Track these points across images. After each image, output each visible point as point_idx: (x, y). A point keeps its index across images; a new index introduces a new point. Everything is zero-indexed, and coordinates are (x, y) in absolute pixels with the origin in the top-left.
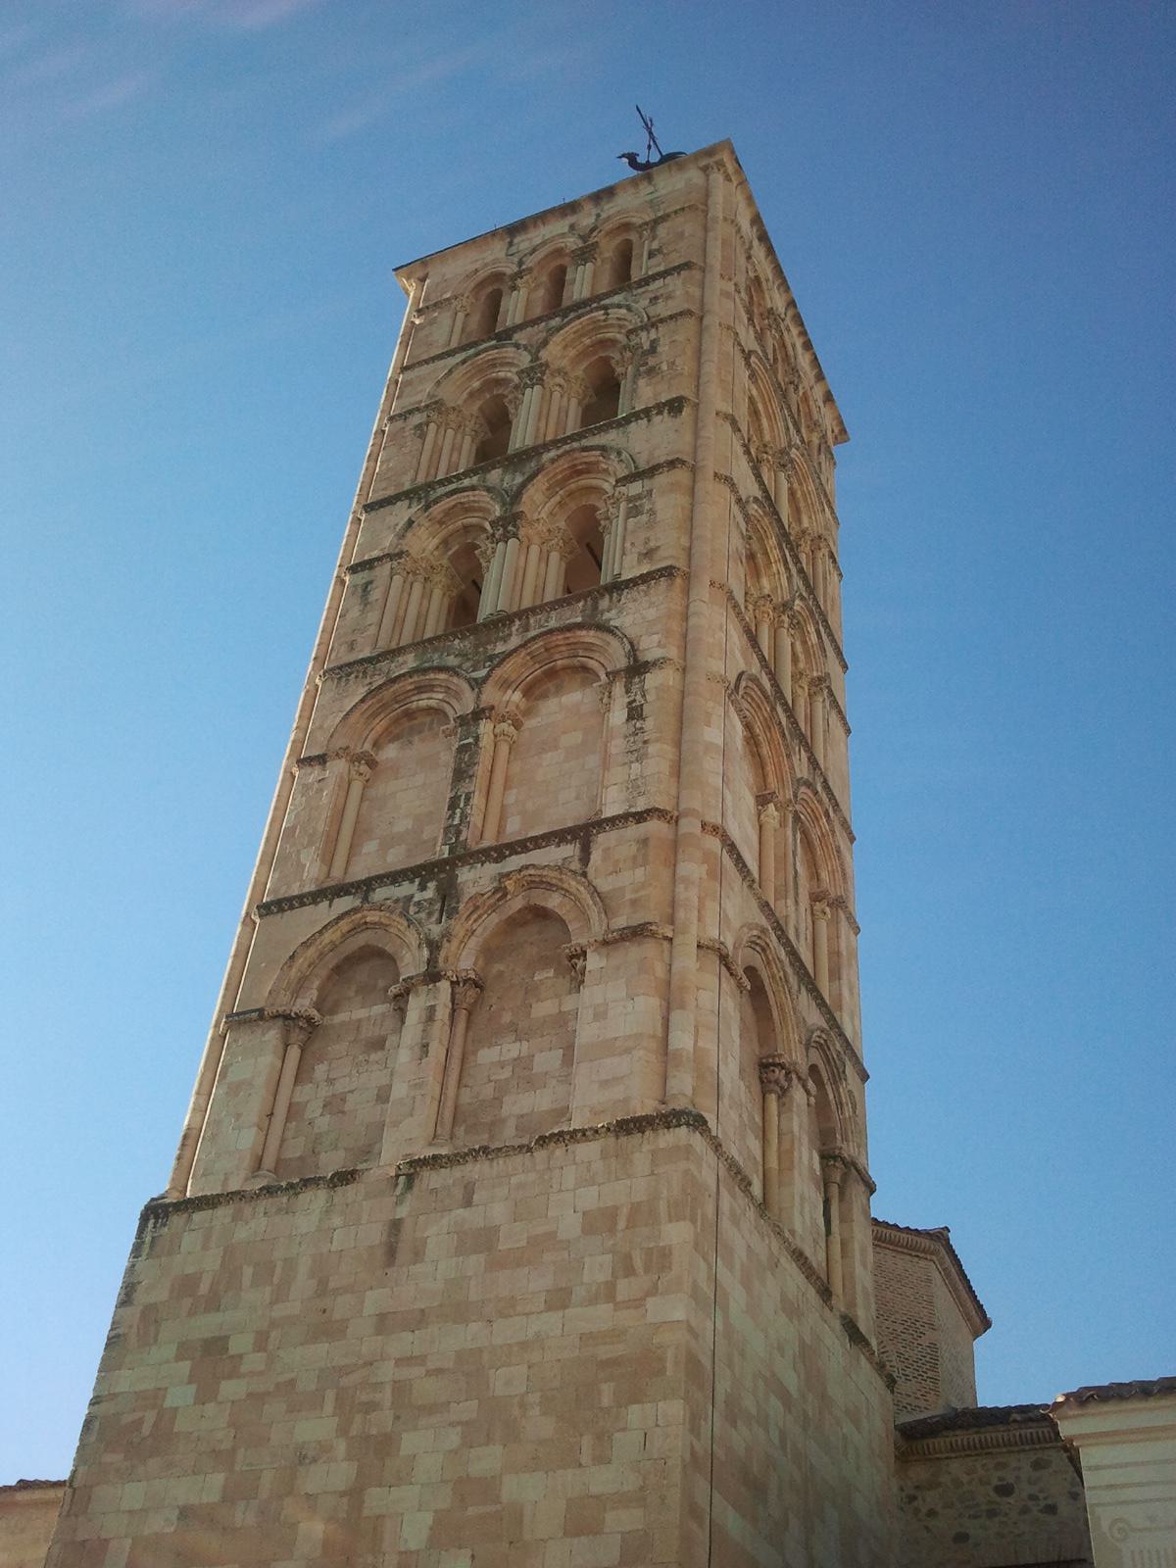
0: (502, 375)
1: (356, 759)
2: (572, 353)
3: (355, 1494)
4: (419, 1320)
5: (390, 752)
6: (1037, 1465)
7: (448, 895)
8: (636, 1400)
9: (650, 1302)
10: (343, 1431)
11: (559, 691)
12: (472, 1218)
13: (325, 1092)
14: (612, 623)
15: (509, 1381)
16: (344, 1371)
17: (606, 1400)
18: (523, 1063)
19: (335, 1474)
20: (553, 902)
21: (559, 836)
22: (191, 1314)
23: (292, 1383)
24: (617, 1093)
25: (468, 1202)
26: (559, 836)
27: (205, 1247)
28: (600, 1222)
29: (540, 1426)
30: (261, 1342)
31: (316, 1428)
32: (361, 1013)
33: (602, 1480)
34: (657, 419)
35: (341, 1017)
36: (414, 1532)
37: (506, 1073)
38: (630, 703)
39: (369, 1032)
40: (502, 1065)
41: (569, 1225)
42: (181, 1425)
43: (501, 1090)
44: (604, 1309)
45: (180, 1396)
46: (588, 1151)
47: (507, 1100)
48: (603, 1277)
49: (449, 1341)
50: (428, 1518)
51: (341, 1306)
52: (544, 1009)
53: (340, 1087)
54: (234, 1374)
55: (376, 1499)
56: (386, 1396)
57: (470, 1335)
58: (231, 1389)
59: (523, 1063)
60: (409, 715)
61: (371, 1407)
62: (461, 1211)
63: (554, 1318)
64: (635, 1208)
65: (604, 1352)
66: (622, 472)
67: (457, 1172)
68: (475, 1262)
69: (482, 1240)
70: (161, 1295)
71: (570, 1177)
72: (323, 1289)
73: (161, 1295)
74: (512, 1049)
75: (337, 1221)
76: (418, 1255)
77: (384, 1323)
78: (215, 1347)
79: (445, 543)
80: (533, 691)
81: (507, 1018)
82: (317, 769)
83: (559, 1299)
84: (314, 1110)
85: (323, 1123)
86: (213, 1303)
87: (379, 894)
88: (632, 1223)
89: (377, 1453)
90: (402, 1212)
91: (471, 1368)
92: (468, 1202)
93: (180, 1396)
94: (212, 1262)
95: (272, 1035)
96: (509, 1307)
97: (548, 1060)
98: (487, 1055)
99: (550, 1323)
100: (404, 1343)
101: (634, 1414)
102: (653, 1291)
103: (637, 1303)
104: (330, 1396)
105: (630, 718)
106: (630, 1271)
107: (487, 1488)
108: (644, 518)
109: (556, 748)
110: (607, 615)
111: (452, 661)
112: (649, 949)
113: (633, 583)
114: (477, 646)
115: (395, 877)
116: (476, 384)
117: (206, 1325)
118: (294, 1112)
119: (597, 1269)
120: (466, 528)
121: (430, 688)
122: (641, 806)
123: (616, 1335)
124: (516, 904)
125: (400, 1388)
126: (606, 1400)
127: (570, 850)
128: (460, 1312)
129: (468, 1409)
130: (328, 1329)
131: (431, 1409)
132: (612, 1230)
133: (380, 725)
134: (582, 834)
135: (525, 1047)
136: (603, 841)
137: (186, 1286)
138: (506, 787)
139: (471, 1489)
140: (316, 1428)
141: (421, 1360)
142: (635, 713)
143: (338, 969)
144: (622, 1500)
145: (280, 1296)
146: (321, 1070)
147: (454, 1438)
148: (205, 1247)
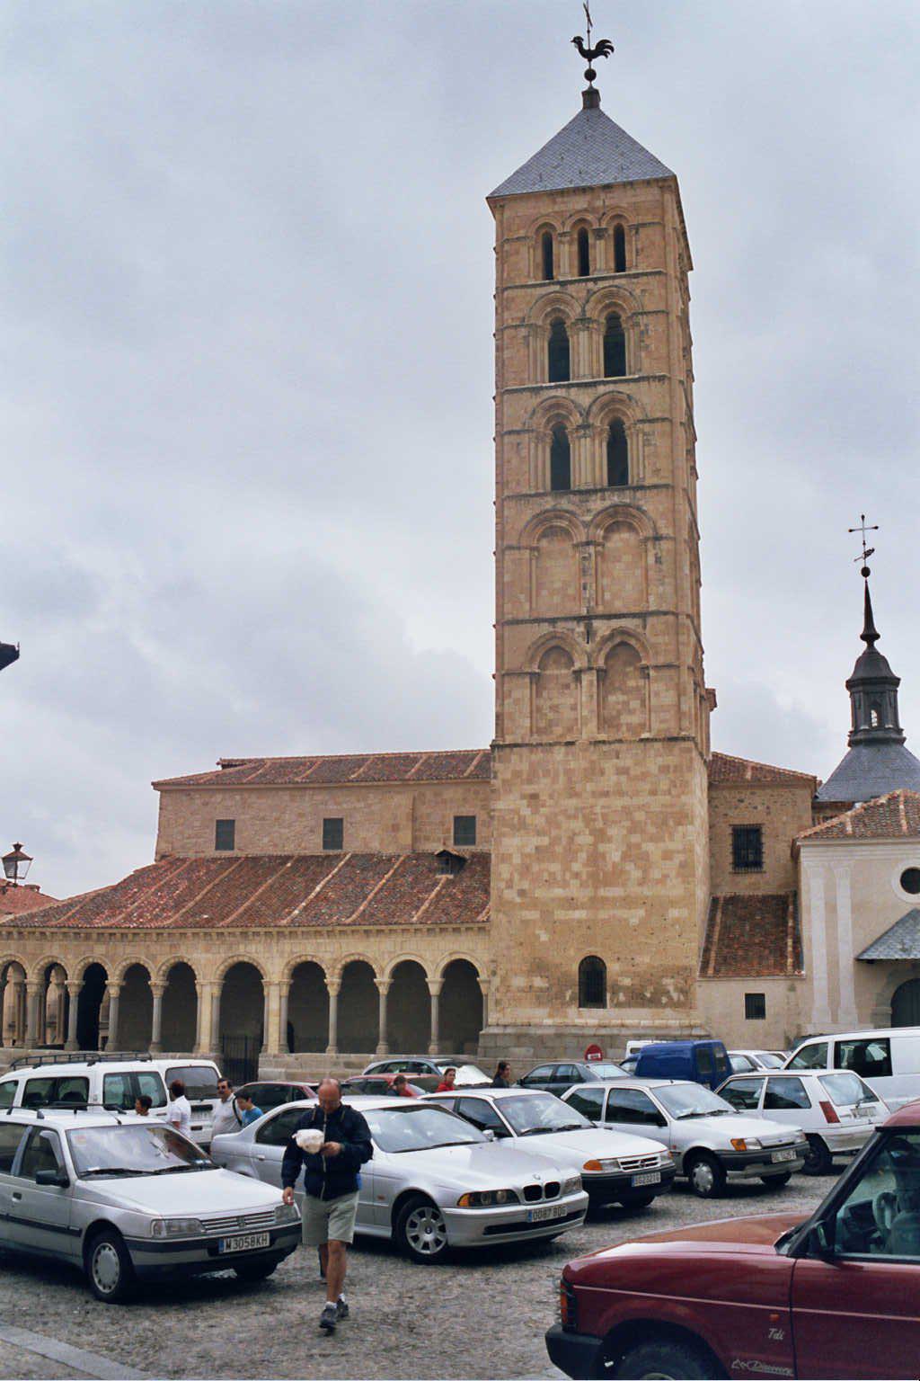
0: (562, 307)
1: (532, 549)
2: (600, 306)
3: (595, 845)
4: (606, 794)
5: (544, 543)
6: (753, 793)
7: (589, 634)
8: (680, 824)
9: (683, 797)
10: (587, 826)
11: (618, 530)
12: (621, 763)
13: (549, 703)
14: (644, 508)
15: (640, 816)
16: (584, 808)
17: (671, 823)
18: (626, 703)
19: (586, 839)
20: (633, 642)
21: (634, 615)
22: (522, 783)
23: (566, 810)
24: (664, 726)
25: (618, 758)
26: (634, 615)
27: (521, 761)
28: (664, 769)
29: (651, 829)
30: (551, 797)
31: (577, 825)
32: (556, 672)
33: (672, 846)
34: (653, 384)
35: (548, 672)
36: (615, 856)
37: (620, 707)
38: (656, 554)
39: (561, 681)
40: (618, 703)
41: (654, 769)
42: (528, 821)
43: (619, 713)
44: (668, 797)
45: (526, 812)
46: (658, 745)
47: (622, 717)
48: (665, 788)
49: (618, 803)
50: (620, 853)
51: (578, 787)
52: (631, 683)
53: (555, 702)
54: (543, 806)
55: (602, 848)
56: (600, 817)
57: (626, 801)
58: (543, 810)
59: (626, 703)
60: (551, 527)
61: (594, 820)
62: (615, 761)
63: (653, 798)
64: (676, 767)
65: (669, 810)
66: (640, 416)
67: (613, 746)
68: (623, 778)
69: (623, 771)
70: (508, 776)
71: (652, 752)
72: (570, 780)
73: (508, 776)
74: (621, 698)
75: (570, 758)
76: (602, 773)
77: (594, 794)
78: (534, 797)
79: (548, 421)
80: (610, 530)
81: (617, 685)
82: (517, 552)
83: (653, 793)
84: (546, 711)
85: (551, 715)
86: (530, 781)
87: (560, 627)
88: (675, 771)
89: (600, 836)
90: (595, 757)
91: (627, 811)
92: (618, 758)
93: (526, 812)
94: (525, 767)
95: (527, 680)
96: (637, 793)
97: (635, 704)
98: (612, 699)
99: (648, 799)
100: (602, 801)
101: (680, 828)
102: (683, 793)
103: (679, 796)
104: (580, 816)
105: (656, 562)
106: (675, 786)
107: (638, 846)
108: (652, 448)
109: (619, 561)
110: (641, 503)
111: (571, 507)
112: (672, 672)
113: (649, 488)
114: (581, 501)
115: (566, 619)
116: (549, 309)
117: (530, 789)
118: (539, 709)
119: (664, 785)
120: (558, 415)
121: (561, 518)
122: (664, 608)
123: (672, 805)
124: (617, 640)
125: (604, 816)
126: (671, 823)
127: (637, 621)
128: (621, 794)
129: (627, 824)
130: (574, 794)
131: (614, 822)
132: (669, 771)
133: (541, 529)
134: (643, 616)
135: (625, 698)
136: (650, 620)
137: (517, 774)
138: (603, 576)
139: (629, 846)
140: (577, 825)
141: (609, 807)
142: (658, 560)
143: (546, 652)
144: (678, 852)
145: (555, 780)
146: (545, 694)
147: (625, 832)
148: (521, 761)
